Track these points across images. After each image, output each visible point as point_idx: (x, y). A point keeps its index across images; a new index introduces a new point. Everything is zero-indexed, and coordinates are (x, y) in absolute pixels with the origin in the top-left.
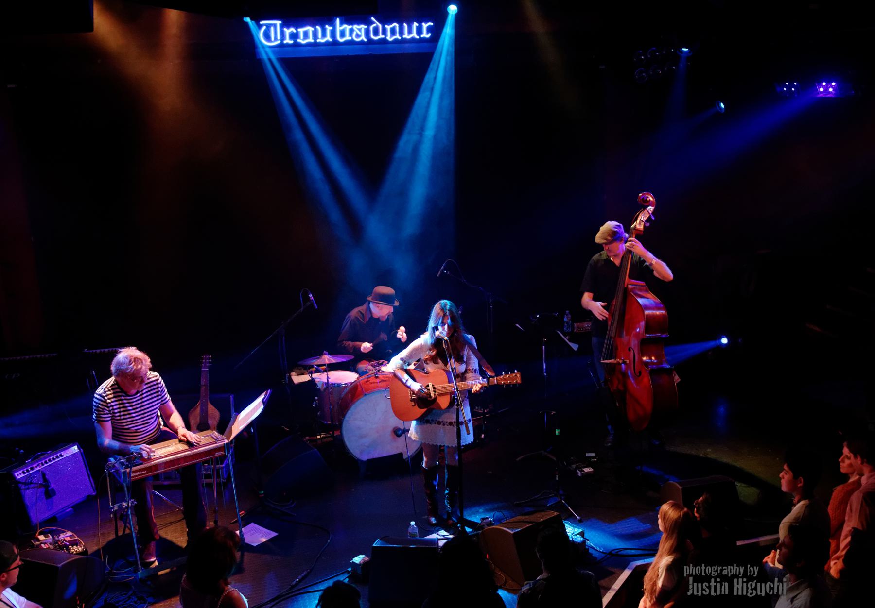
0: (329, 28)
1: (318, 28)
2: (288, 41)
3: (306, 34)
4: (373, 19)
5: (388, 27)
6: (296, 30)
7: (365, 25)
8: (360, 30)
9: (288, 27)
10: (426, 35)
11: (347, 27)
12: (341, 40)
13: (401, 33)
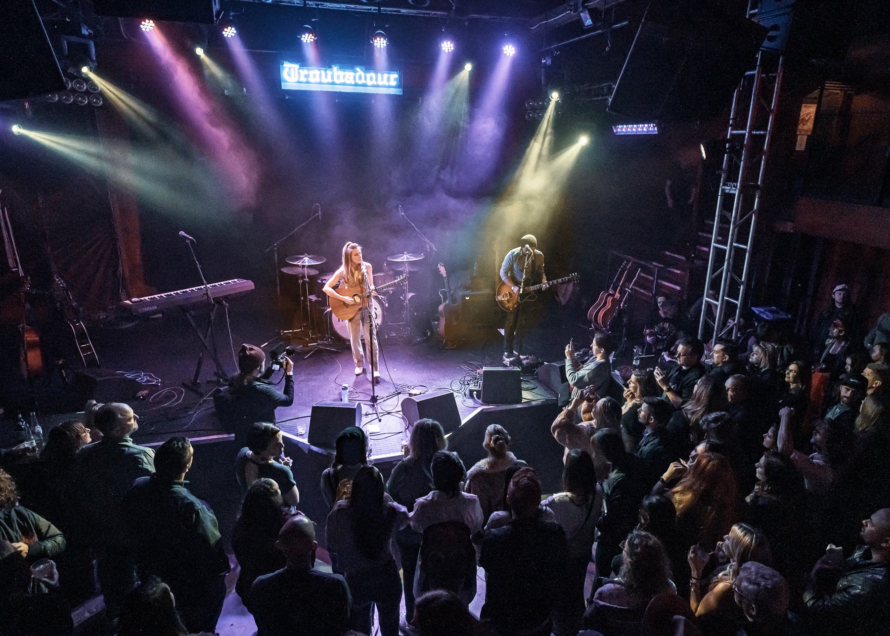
1: (323, 72)
2: (303, 79)
3: (314, 76)
4: (358, 69)
5: (368, 75)
7: (353, 71)
8: (350, 76)
9: (303, 69)
10: (394, 83)
11: (341, 73)
12: (337, 82)
13: (377, 80)
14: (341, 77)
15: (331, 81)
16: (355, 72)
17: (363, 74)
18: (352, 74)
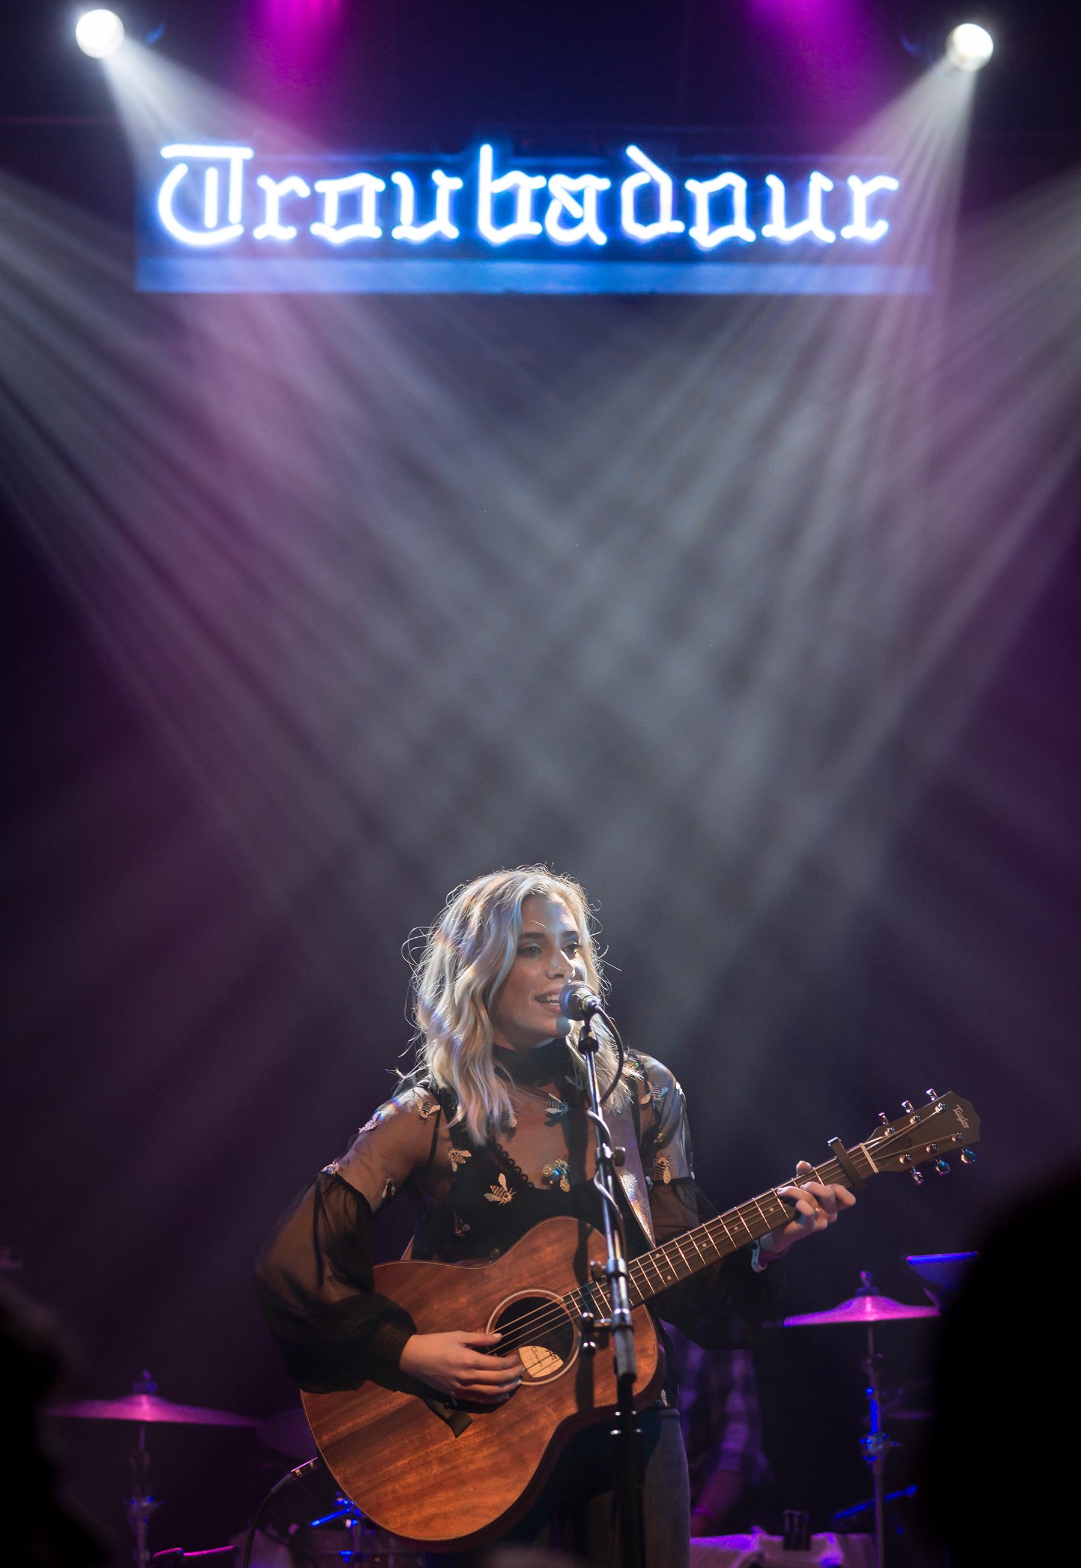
0: (446, 184)
1: (401, 179)
4: (634, 153)
5: (701, 190)
6: (311, 184)
7: (600, 172)
8: (579, 197)
13: (758, 212)
14: (524, 206)
15: (452, 233)
16: (620, 170)
17: (665, 183)
18: (594, 184)
